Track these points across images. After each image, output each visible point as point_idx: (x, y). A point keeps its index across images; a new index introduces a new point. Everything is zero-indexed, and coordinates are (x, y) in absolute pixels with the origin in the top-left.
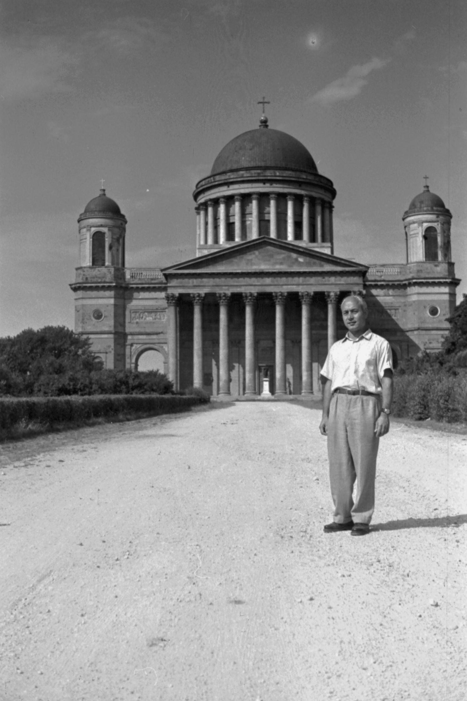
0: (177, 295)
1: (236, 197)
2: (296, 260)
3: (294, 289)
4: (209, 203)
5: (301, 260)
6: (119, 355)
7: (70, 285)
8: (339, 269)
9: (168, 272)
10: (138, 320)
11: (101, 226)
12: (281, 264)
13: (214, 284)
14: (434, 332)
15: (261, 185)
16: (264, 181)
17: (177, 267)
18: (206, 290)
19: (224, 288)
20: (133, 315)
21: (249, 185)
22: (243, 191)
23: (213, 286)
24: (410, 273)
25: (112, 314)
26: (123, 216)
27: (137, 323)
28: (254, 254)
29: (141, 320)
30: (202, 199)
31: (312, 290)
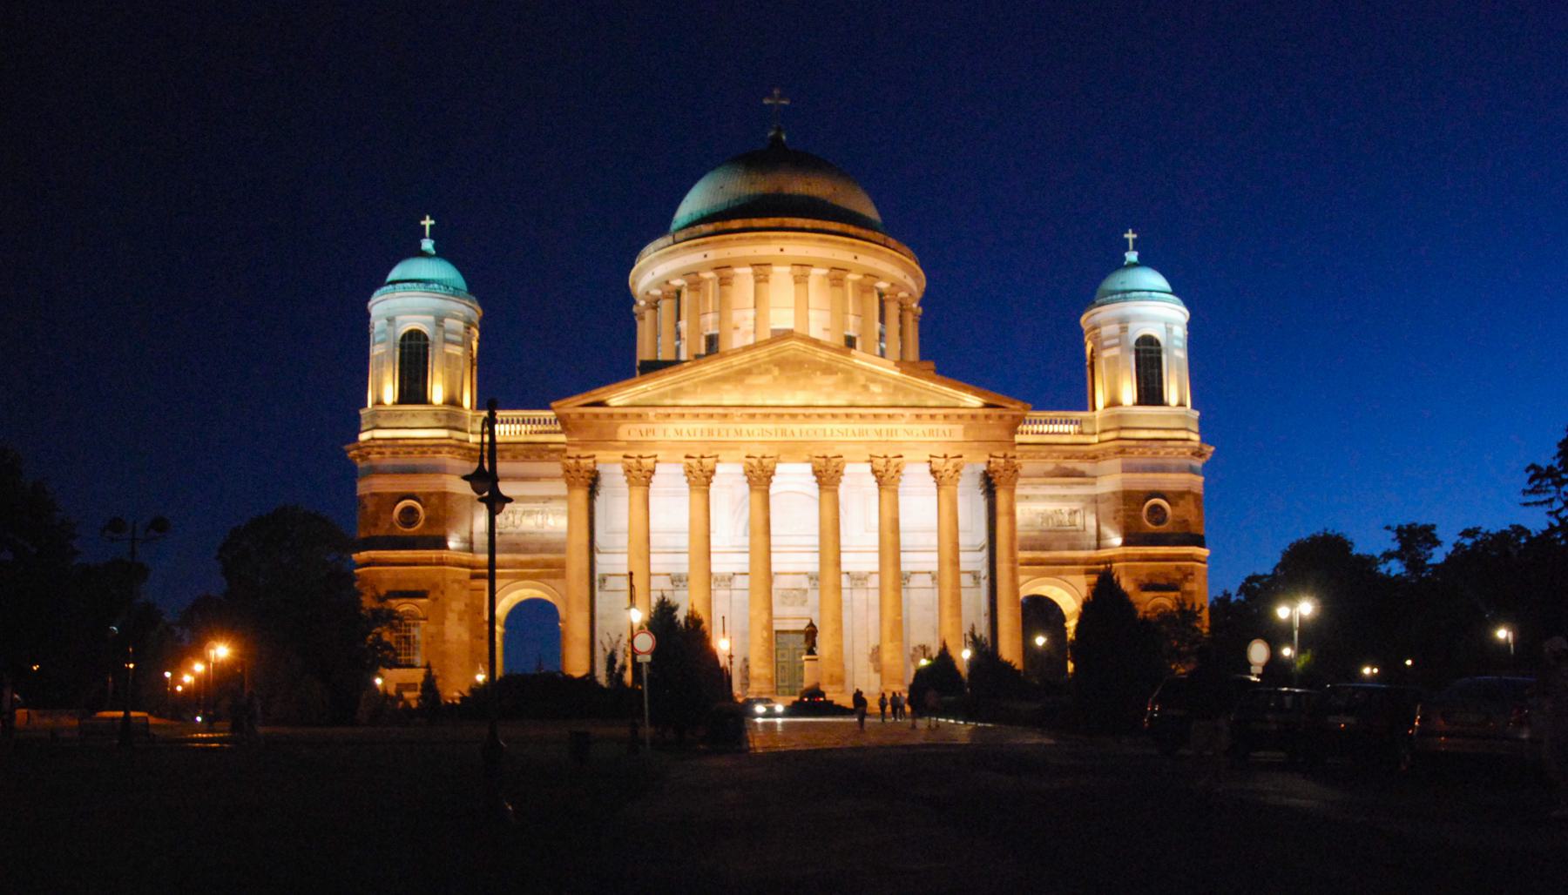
2: (865, 387)
12: (829, 395)
28: (767, 371)
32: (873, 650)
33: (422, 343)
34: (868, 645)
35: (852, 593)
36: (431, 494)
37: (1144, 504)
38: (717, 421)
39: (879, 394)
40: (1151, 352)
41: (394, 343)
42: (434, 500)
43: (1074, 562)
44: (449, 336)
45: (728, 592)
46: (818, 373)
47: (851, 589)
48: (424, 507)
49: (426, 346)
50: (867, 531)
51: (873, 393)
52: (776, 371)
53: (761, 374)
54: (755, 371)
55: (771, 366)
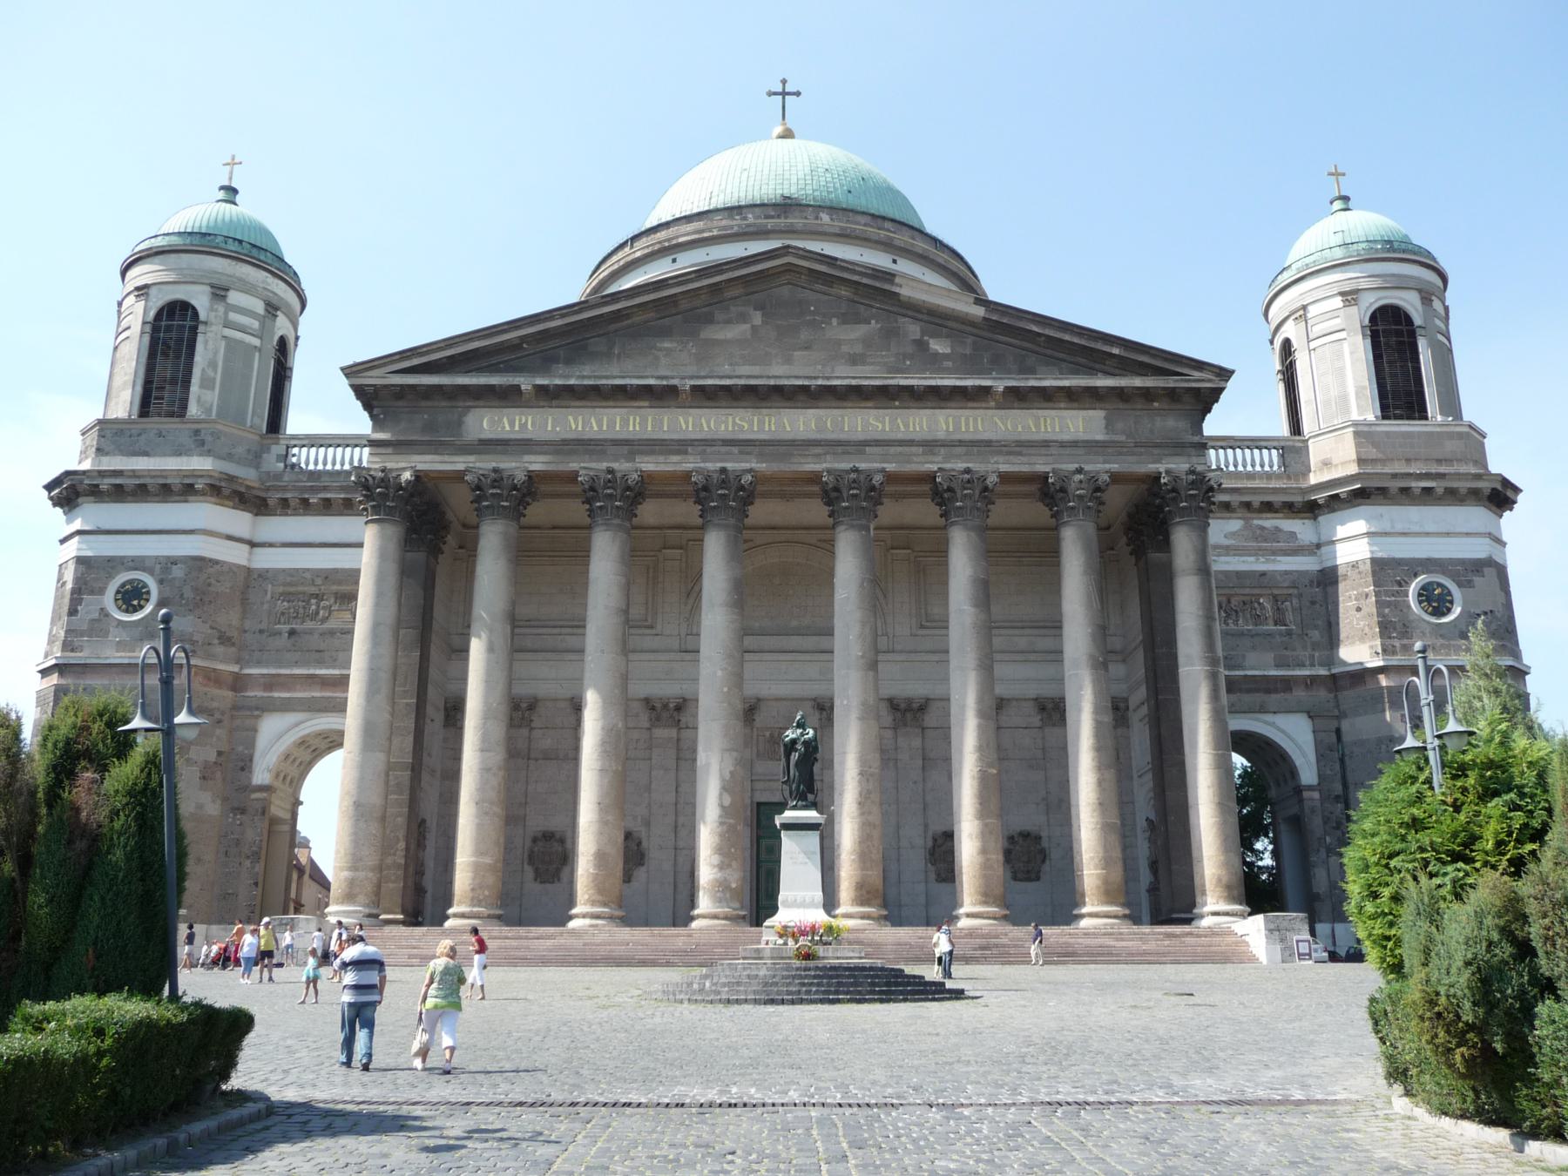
2: (921, 345)
5: (939, 346)
7: (49, 487)
9: (372, 379)
12: (854, 360)
17: (416, 361)
25: (188, 593)
27: (292, 633)
28: (743, 318)
29: (309, 625)
32: (935, 840)
33: (188, 323)
34: (926, 832)
35: (896, 738)
36: (174, 561)
37: (1408, 584)
38: (646, 404)
39: (946, 357)
40: (1399, 333)
41: (144, 323)
42: (178, 572)
43: (1286, 684)
44: (233, 316)
45: (673, 733)
46: (834, 321)
47: (895, 729)
48: (161, 582)
49: (194, 331)
50: (922, 627)
51: (936, 354)
52: (757, 318)
53: (728, 322)
54: (719, 316)
55: (751, 311)
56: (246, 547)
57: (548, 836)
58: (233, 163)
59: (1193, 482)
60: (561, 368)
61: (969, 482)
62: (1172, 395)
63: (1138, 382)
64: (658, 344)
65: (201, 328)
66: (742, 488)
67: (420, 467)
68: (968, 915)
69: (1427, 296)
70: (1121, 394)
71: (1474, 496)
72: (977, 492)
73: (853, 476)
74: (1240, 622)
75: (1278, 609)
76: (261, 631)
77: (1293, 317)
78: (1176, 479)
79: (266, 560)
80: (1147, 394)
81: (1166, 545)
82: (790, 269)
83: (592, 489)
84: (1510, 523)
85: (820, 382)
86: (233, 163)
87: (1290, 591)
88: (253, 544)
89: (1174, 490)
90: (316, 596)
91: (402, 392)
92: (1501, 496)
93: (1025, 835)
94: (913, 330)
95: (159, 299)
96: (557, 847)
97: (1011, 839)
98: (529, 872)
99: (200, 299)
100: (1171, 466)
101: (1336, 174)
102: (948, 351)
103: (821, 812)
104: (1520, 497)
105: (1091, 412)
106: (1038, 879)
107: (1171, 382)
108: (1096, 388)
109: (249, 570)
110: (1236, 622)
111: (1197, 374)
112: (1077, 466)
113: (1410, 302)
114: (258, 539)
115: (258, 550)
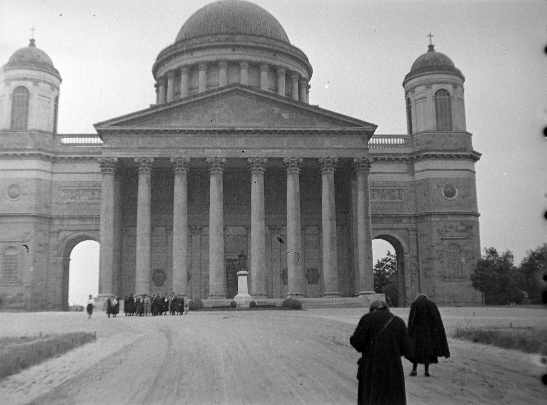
0: (116, 159)
1: (200, 66)
2: (279, 115)
3: (276, 153)
4: (170, 74)
5: (285, 116)
6: (40, 245)
8: (337, 129)
9: (102, 128)
10: (69, 200)
11: (25, 79)
13: (168, 146)
14: (450, 218)
15: (230, 51)
16: (234, 47)
17: (116, 122)
18: (156, 154)
19: (180, 151)
20: (63, 194)
21: (216, 51)
22: (209, 59)
23: (166, 148)
24: (418, 145)
26: (57, 72)
28: (221, 106)
30: (161, 73)
31: (301, 154)
39: (287, 119)
51: (284, 118)
52: (226, 106)
56: (50, 174)
57: (158, 271)
58: (33, 30)
59: (364, 161)
60: (163, 124)
61: (294, 161)
62: (359, 133)
63: (348, 129)
64: (195, 115)
65: (30, 96)
66: (222, 163)
67: (119, 156)
68: (291, 295)
69: (455, 86)
70: (342, 133)
71: (466, 157)
72: (296, 165)
73: (257, 159)
74: (387, 198)
75: (400, 194)
76: (57, 203)
77: (411, 91)
78: (359, 160)
79: (56, 178)
80: (350, 133)
81: (356, 179)
82: (237, 89)
83: (175, 163)
84: (477, 164)
85: (247, 129)
86: (33, 30)
87: (403, 188)
88: (52, 173)
89: (358, 163)
90: (75, 190)
91: (113, 132)
92: (475, 157)
93: (313, 270)
94: (277, 110)
95: (15, 84)
96: (161, 274)
97: (308, 271)
98: (153, 283)
99: (29, 85)
100: (358, 156)
101: (430, 36)
102: (288, 117)
103: (247, 271)
104: (482, 157)
105: (333, 138)
106: (317, 283)
107: (359, 129)
108: (334, 131)
109: (51, 182)
110: (385, 199)
111: (367, 127)
112: (327, 156)
113: (449, 88)
114: (54, 171)
115: (54, 175)
